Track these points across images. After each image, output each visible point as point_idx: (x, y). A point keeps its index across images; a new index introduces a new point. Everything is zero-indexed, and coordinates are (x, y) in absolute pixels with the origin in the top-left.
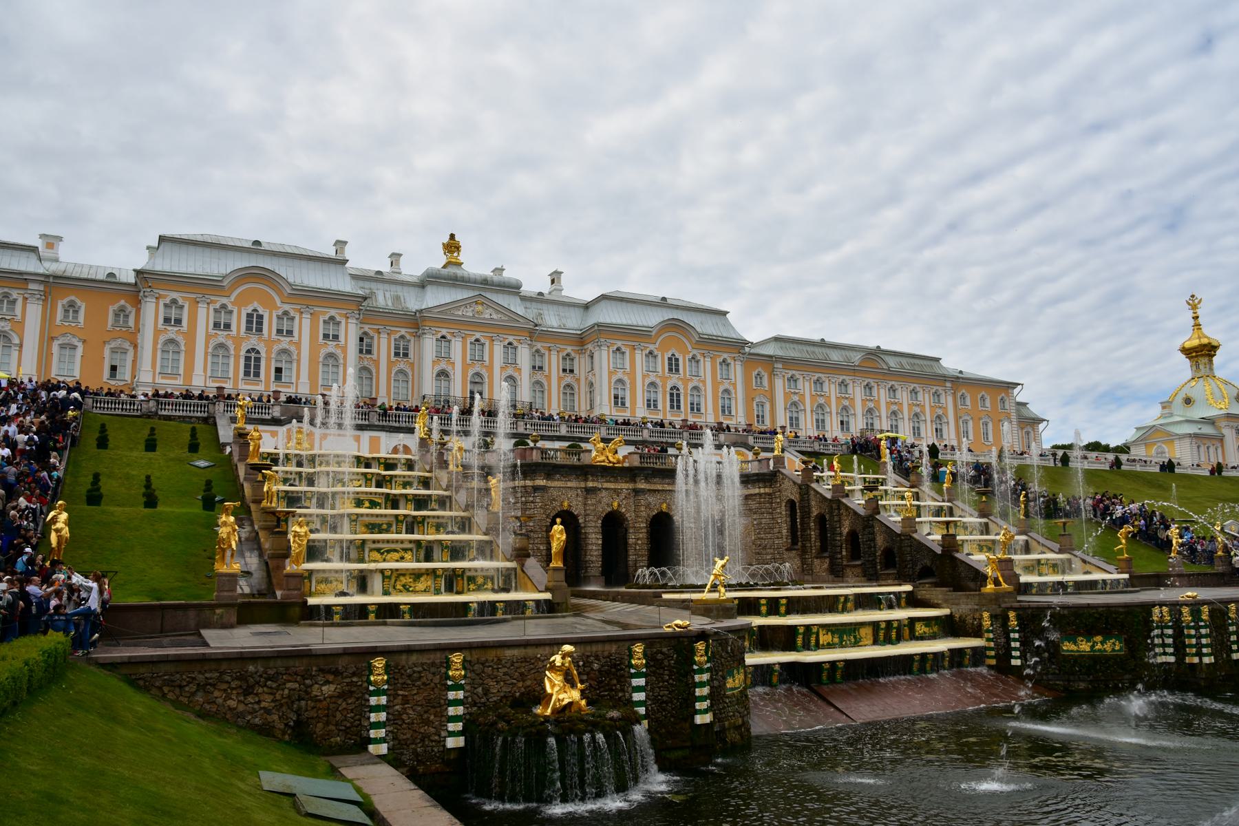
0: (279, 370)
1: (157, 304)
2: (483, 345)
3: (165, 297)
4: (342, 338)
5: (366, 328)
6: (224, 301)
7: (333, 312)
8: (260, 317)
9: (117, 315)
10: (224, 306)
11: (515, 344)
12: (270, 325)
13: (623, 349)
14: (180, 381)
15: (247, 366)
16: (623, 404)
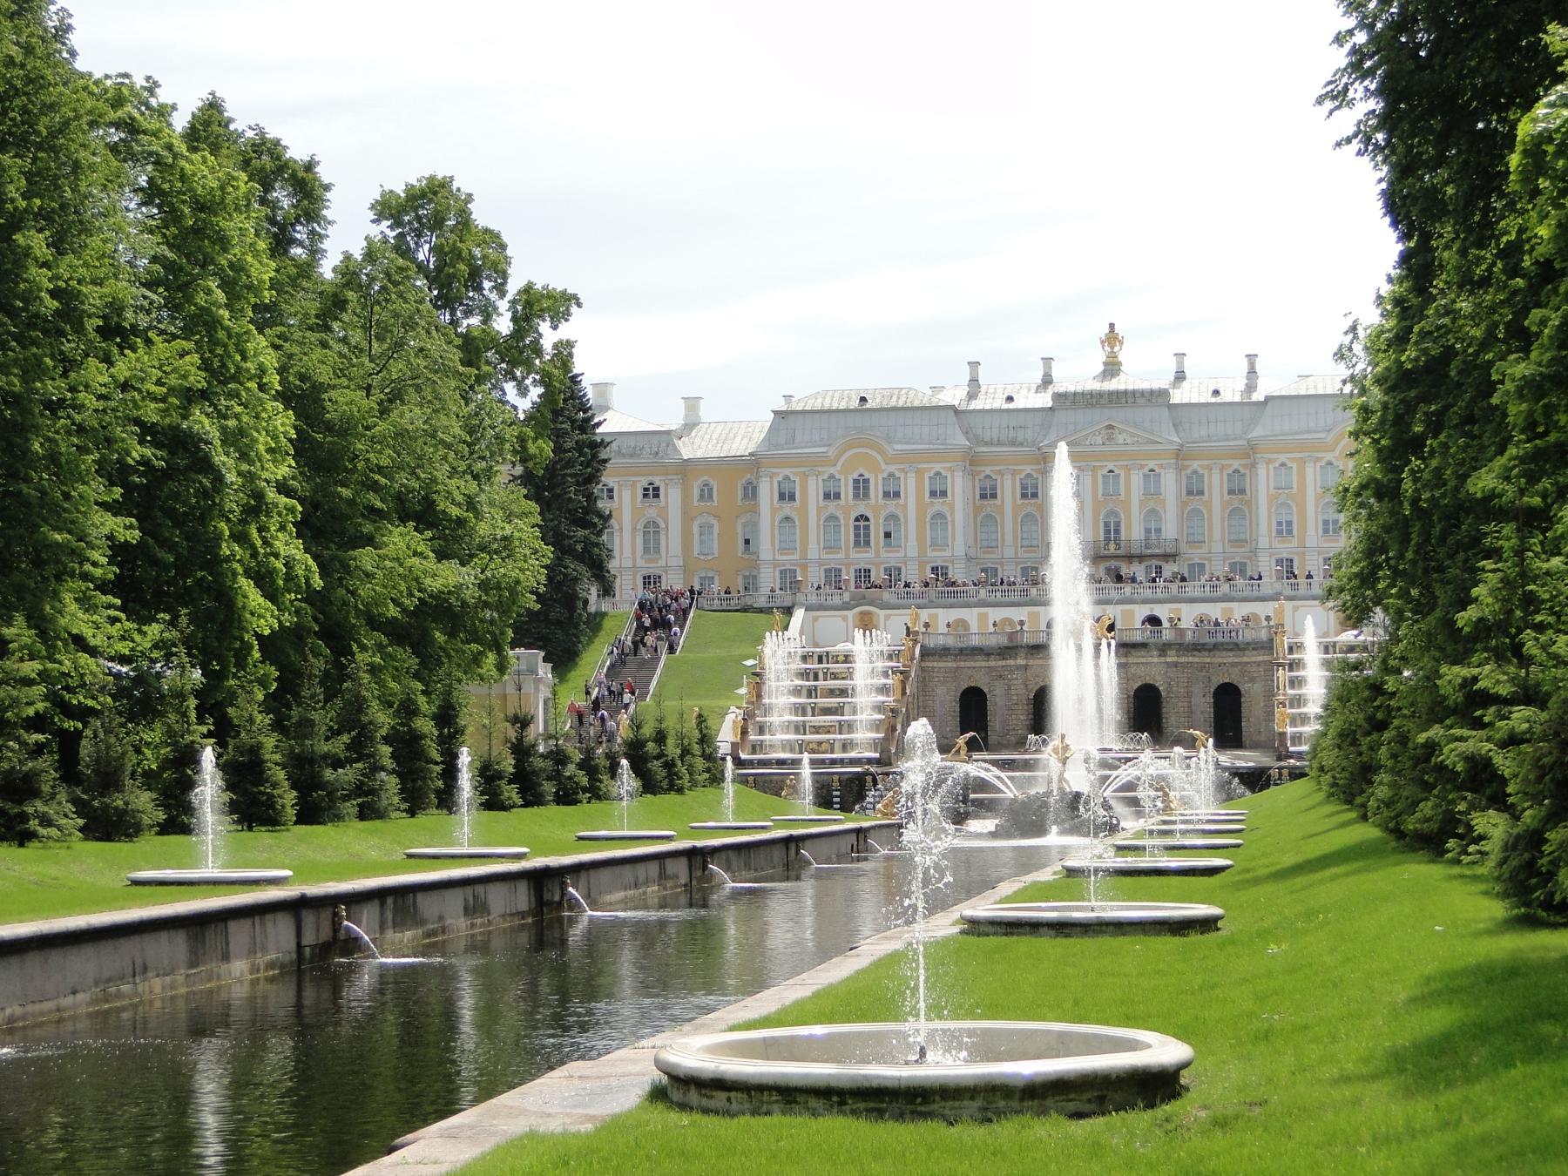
0: (888, 535)
1: (772, 482)
2: (1118, 476)
3: (778, 474)
4: (949, 494)
5: (988, 473)
6: (832, 470)
7: (938, 467)
8: (866, 481)
9: (745, 489)
10: (832, 477)
11: (1156, 468)
12: (876, 490)
13: (1289, 464)
14: (796, 557)
15: (857, 535)
16: (1290, 532)
